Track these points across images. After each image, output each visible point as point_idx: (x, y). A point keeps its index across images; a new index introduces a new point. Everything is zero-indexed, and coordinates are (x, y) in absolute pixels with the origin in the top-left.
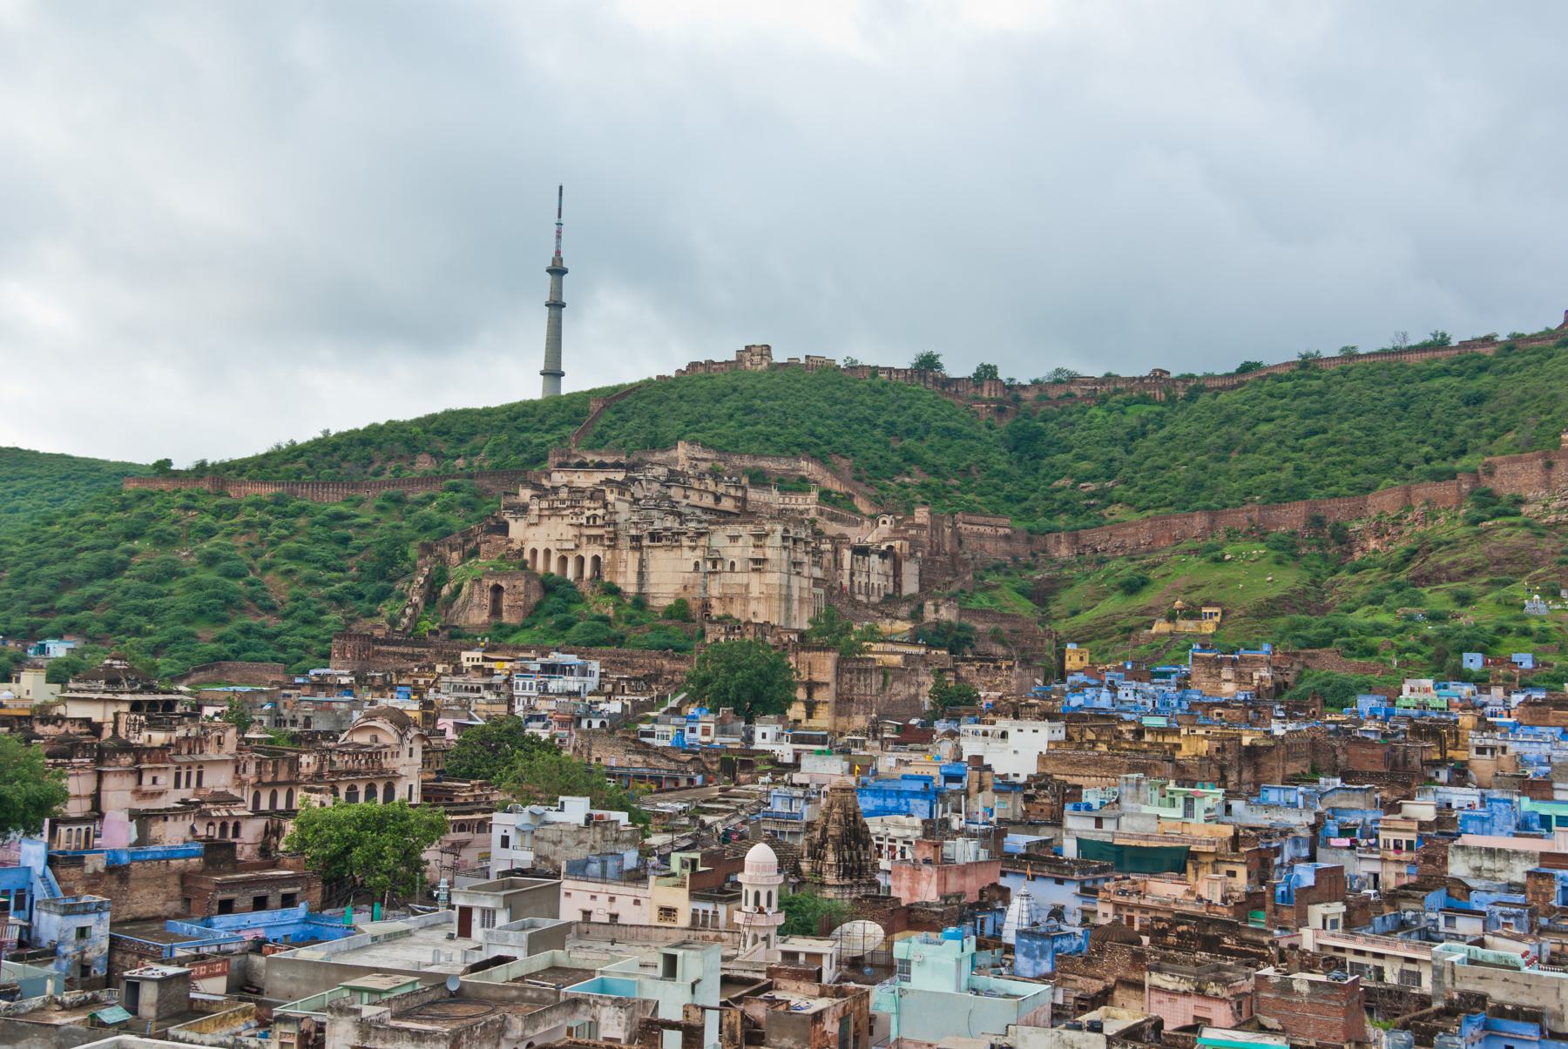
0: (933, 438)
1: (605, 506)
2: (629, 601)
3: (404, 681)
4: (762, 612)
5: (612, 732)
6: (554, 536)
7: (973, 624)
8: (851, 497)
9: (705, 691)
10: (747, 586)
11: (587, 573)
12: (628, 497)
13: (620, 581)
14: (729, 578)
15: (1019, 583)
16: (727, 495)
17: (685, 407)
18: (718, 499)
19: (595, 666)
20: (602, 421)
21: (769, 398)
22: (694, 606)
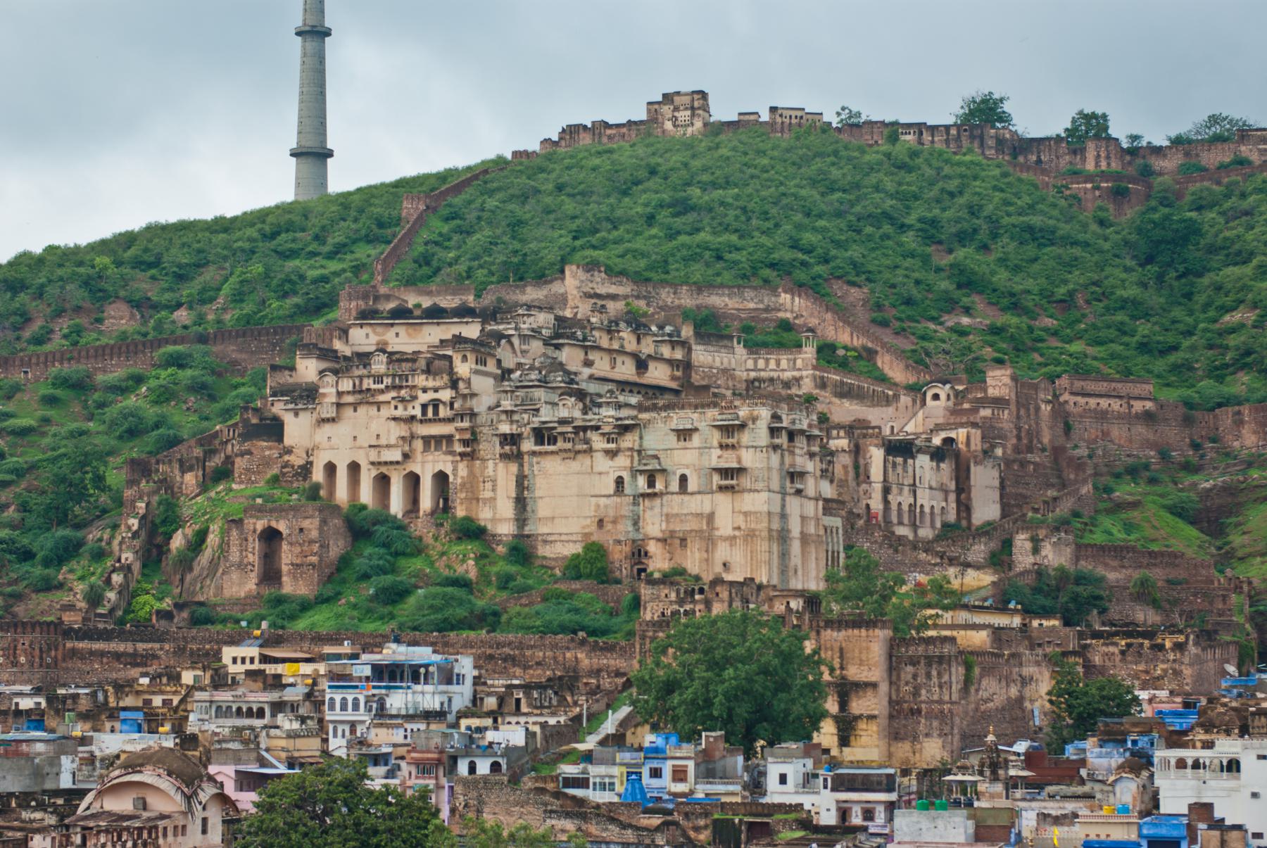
0: (1006, 245)
1: (454, 384)
2: (501, 549)
3: (129, 701)
4: (740, 563)
5: (515, 780)
6: (364, 440)
7: (1100, 571)
8: (870, 354)
9: (667, 706)
10: (711, 517)
11: (426, 502)
12: (491, 367)
13: (484, 516)
14: (676, 504)
15: (1174, 497)
16: (658, 358)
17: (570, 206)
18: (642, 365)
19: (466, 665)
20: (425, 234)
21: (714, 185)
22: (618, 555)
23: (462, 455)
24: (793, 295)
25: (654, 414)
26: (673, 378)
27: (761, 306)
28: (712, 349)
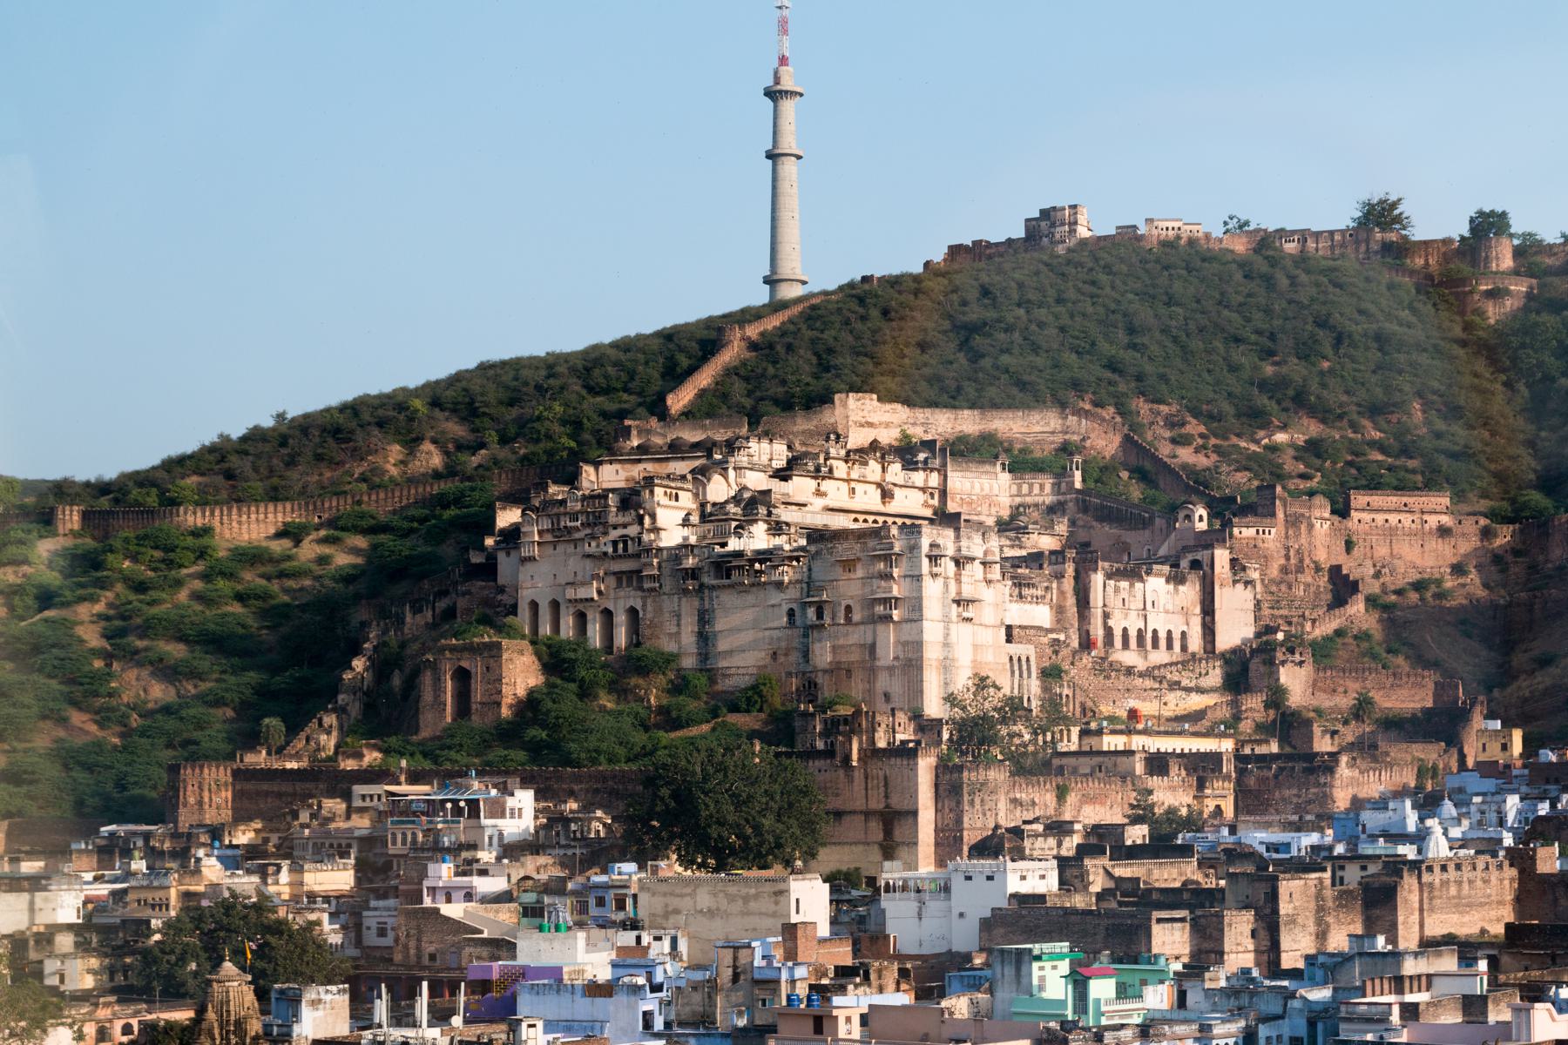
10: (872, 648)
26: (926, 505)
28: (968, 474)
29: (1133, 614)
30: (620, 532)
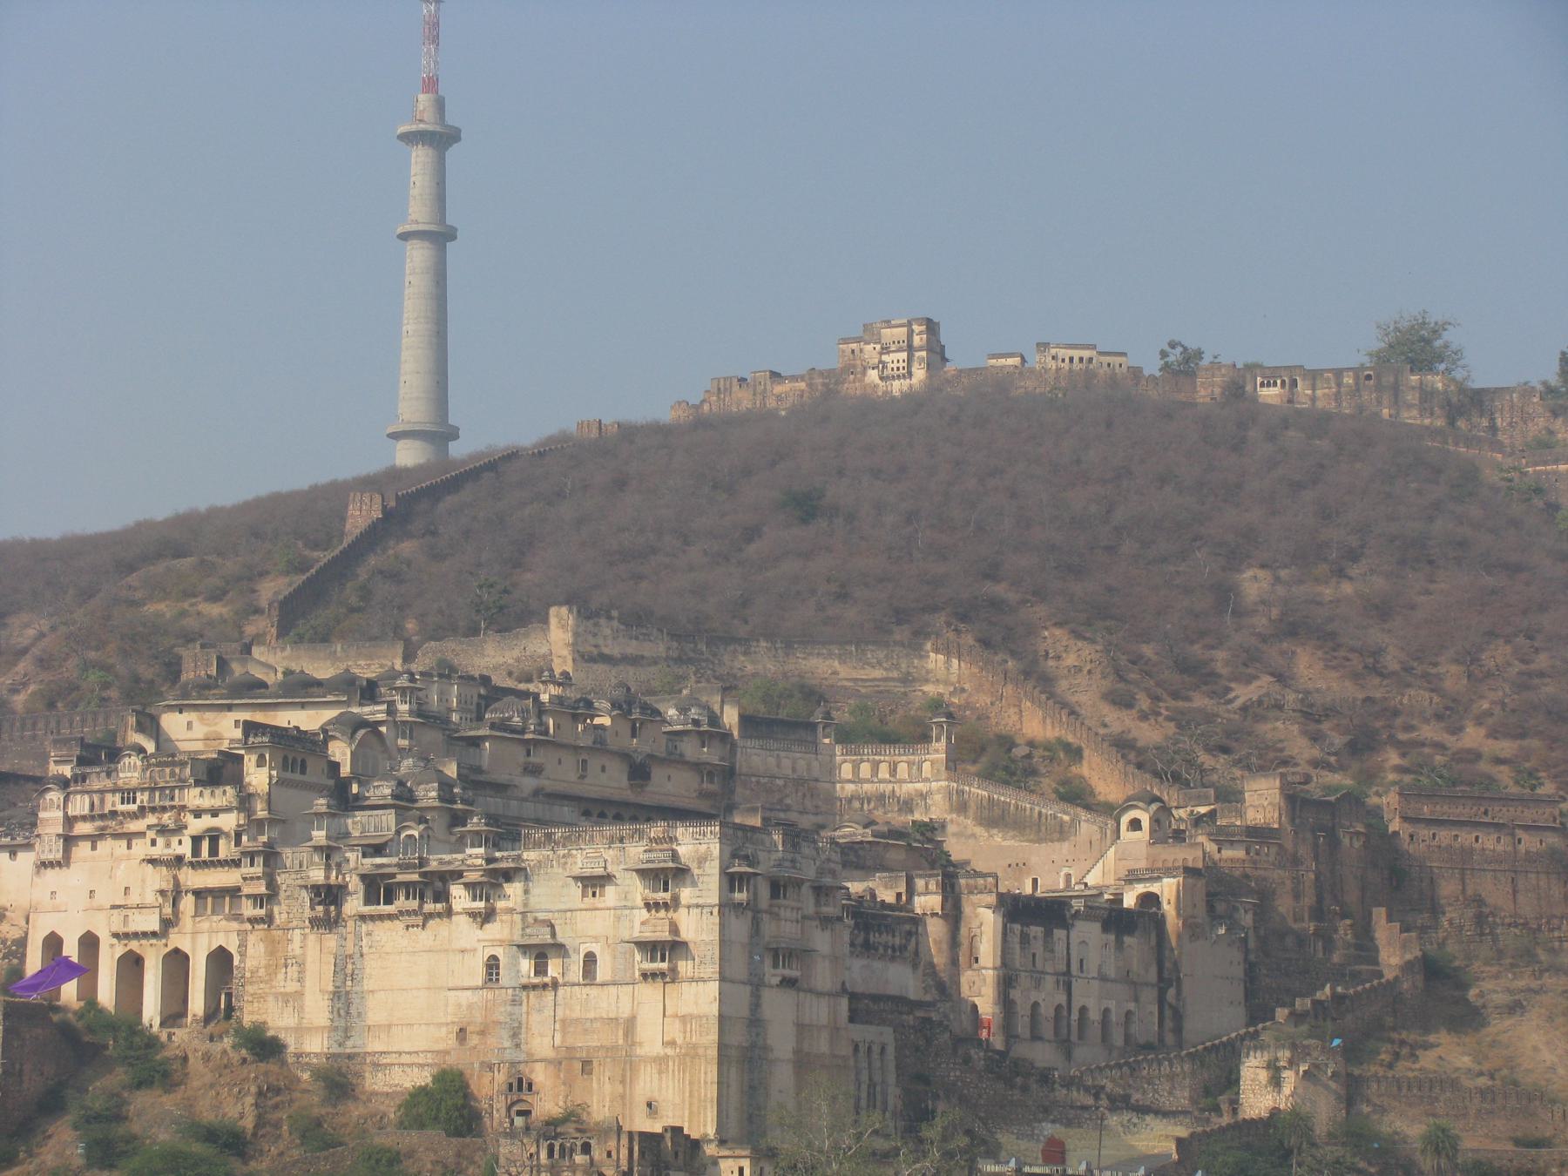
6: (106, 897)
10: (630, 1025)
11: (197, 1003)
13: (279, 1021)
14: (582, 1002)
18: (639, 772)
22: (488, 1088)
23: (253, 921)
24: (948, 654)
25: (547, 852)
26: (703, 795)
27: (895, 674)
29: (1049, 982)
30: (207, 822)
